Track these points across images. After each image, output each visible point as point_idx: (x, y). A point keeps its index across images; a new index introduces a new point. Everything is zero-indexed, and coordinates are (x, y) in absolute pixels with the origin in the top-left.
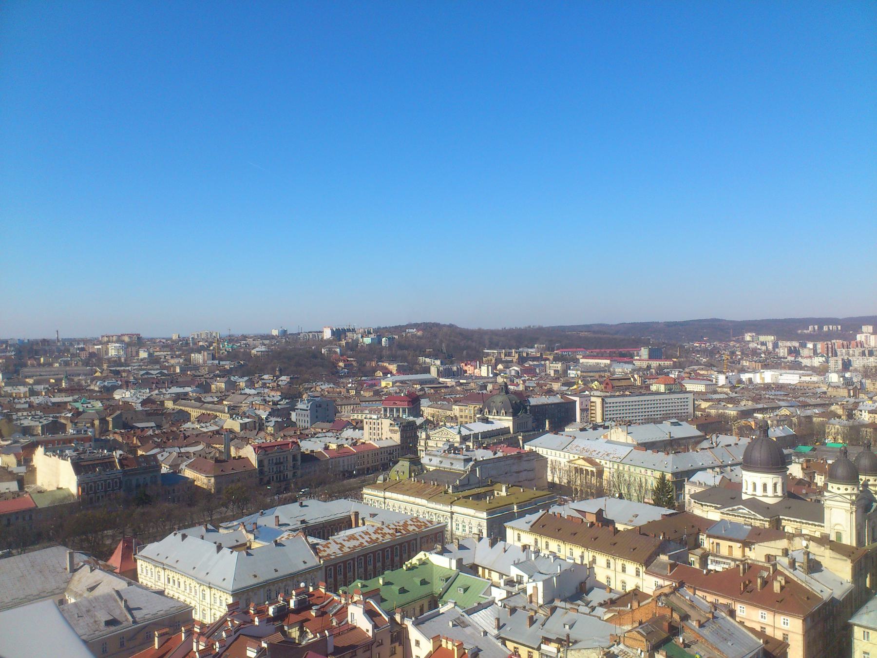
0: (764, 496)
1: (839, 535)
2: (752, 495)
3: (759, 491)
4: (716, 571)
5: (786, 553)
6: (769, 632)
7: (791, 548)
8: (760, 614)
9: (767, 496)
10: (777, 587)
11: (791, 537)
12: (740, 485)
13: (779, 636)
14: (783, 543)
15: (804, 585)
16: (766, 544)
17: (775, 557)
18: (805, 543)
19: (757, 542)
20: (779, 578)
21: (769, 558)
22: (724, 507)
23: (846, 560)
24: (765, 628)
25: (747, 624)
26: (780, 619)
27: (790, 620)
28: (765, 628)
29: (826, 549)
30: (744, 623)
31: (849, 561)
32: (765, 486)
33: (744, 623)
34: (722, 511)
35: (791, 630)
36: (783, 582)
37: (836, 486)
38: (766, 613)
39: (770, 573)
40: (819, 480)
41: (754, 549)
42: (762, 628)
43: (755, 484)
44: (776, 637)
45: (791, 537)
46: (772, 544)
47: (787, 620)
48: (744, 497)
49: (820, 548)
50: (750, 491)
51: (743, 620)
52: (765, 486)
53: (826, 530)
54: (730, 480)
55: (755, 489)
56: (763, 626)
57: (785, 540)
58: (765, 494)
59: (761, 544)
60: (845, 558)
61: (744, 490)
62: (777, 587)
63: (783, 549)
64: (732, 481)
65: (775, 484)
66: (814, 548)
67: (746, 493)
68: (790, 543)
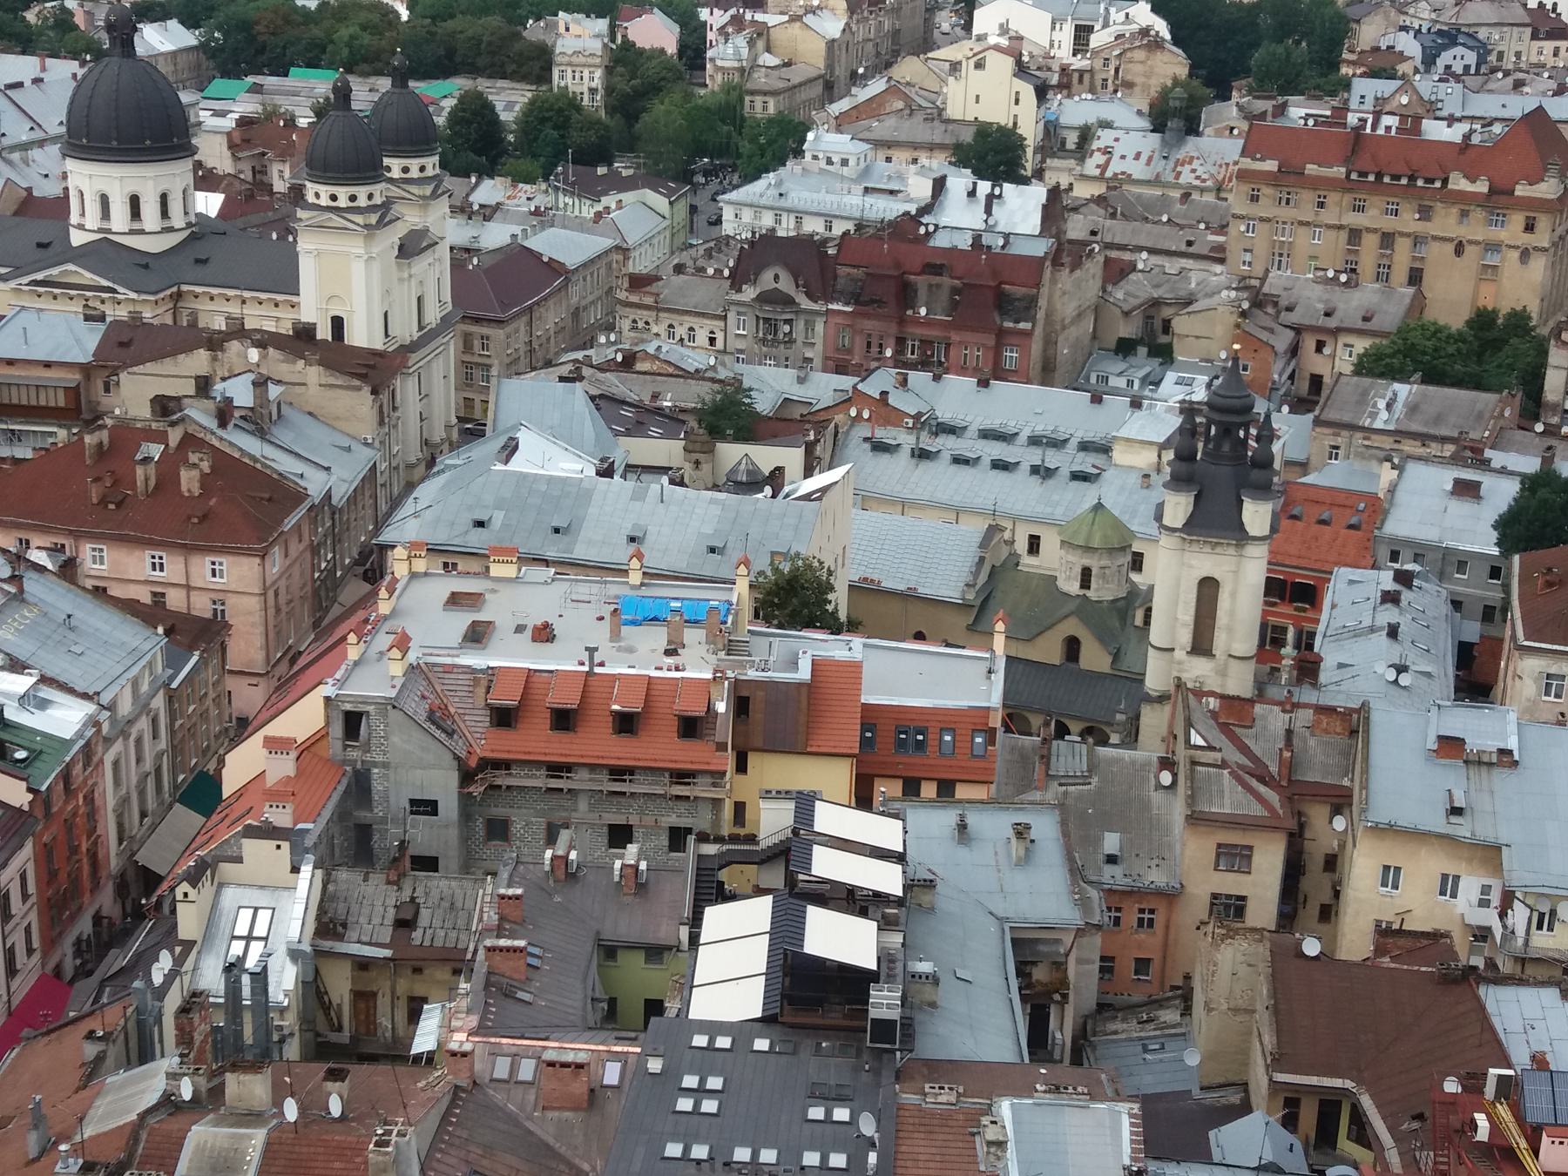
0: (132, 232)
1: (338, 324)
2: (100, 231)
3: (120, 219)
4: (16, 461)
5: (204, 385)
6: (175, 600)
7: (220, 374)
8: (149, 561)
9: (142, 232)
10: (189, 481)
11: (215, 343)
12: (59, 207)
13: (202, 606)
14: (198, 362)
15: (258, 466)
16: (149, 367)
17: (178, 399)
18: (254, 354)
19: (125, 366)
20: (193, 458)
21: (164, 406)
22: (18, 271)
23: (359, 389)
24: (163, 595)
25: (116, 591)
26: (201, 567)
27: (225, 562)
28: (163, 595)
29: (309, 363)
30: (105, 589)
31: (367, 390)
32: (135, 202)
33: (105, 589)
34: (12, 284)
35: (233, 587)
36: (205, 466)
37: (325, 191)
38: (164, 555)
39: (167, 445)
40: (280, 178)
41: (118, 383)
42: (155, 594)
43: (104, 201)
44: (194, 613)
45: (215, 343)
46: (166, 366)
47: (221, 564)
48: (77, 238)
49: (294, 362)
50: (93, 220)
51: (101, 584)
52: (135, 202)
53: (308, 314)
54: (29, 190)
55: (106, 213)
56: (159, 589)
57: (201, 351)
58: (136, 226)
59: (135, 369)
60: (357, 383)
61: (74, 218)
62: (189, 481)
63: (197, 378)
64: (35, 193)
65: (164, 198)
66: (277, 364)
67: (81, 227)
68: (215, 359)
